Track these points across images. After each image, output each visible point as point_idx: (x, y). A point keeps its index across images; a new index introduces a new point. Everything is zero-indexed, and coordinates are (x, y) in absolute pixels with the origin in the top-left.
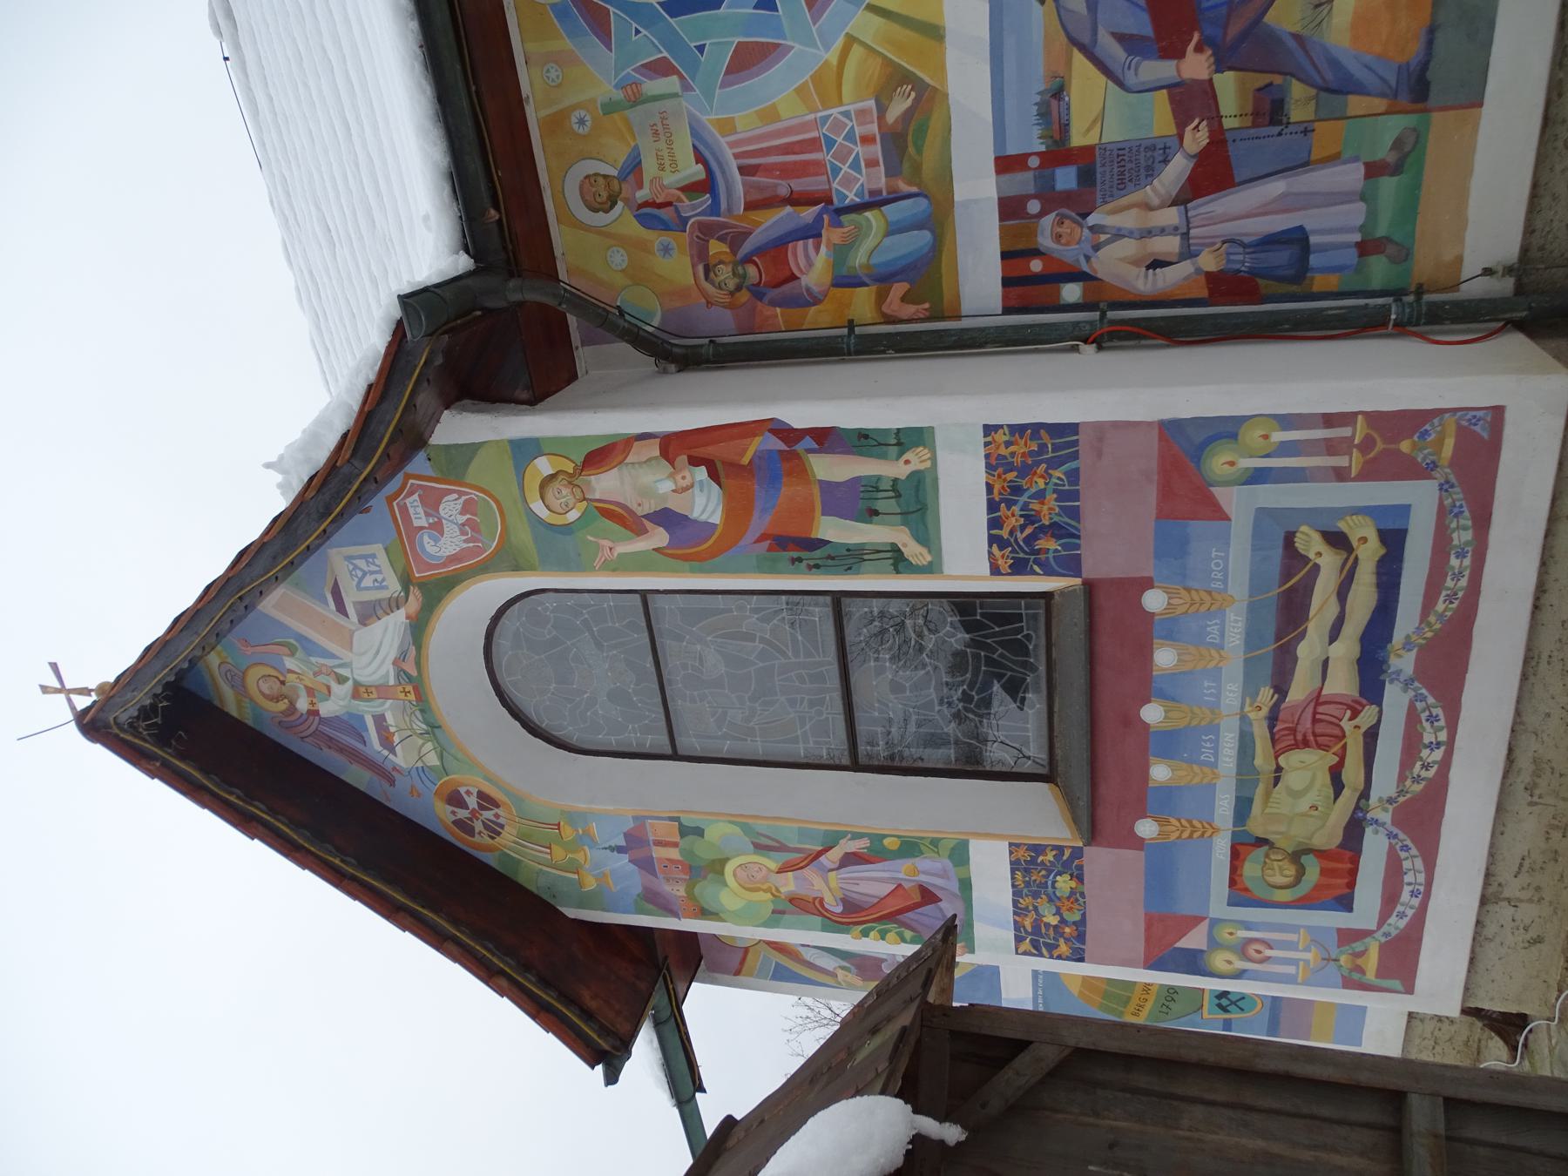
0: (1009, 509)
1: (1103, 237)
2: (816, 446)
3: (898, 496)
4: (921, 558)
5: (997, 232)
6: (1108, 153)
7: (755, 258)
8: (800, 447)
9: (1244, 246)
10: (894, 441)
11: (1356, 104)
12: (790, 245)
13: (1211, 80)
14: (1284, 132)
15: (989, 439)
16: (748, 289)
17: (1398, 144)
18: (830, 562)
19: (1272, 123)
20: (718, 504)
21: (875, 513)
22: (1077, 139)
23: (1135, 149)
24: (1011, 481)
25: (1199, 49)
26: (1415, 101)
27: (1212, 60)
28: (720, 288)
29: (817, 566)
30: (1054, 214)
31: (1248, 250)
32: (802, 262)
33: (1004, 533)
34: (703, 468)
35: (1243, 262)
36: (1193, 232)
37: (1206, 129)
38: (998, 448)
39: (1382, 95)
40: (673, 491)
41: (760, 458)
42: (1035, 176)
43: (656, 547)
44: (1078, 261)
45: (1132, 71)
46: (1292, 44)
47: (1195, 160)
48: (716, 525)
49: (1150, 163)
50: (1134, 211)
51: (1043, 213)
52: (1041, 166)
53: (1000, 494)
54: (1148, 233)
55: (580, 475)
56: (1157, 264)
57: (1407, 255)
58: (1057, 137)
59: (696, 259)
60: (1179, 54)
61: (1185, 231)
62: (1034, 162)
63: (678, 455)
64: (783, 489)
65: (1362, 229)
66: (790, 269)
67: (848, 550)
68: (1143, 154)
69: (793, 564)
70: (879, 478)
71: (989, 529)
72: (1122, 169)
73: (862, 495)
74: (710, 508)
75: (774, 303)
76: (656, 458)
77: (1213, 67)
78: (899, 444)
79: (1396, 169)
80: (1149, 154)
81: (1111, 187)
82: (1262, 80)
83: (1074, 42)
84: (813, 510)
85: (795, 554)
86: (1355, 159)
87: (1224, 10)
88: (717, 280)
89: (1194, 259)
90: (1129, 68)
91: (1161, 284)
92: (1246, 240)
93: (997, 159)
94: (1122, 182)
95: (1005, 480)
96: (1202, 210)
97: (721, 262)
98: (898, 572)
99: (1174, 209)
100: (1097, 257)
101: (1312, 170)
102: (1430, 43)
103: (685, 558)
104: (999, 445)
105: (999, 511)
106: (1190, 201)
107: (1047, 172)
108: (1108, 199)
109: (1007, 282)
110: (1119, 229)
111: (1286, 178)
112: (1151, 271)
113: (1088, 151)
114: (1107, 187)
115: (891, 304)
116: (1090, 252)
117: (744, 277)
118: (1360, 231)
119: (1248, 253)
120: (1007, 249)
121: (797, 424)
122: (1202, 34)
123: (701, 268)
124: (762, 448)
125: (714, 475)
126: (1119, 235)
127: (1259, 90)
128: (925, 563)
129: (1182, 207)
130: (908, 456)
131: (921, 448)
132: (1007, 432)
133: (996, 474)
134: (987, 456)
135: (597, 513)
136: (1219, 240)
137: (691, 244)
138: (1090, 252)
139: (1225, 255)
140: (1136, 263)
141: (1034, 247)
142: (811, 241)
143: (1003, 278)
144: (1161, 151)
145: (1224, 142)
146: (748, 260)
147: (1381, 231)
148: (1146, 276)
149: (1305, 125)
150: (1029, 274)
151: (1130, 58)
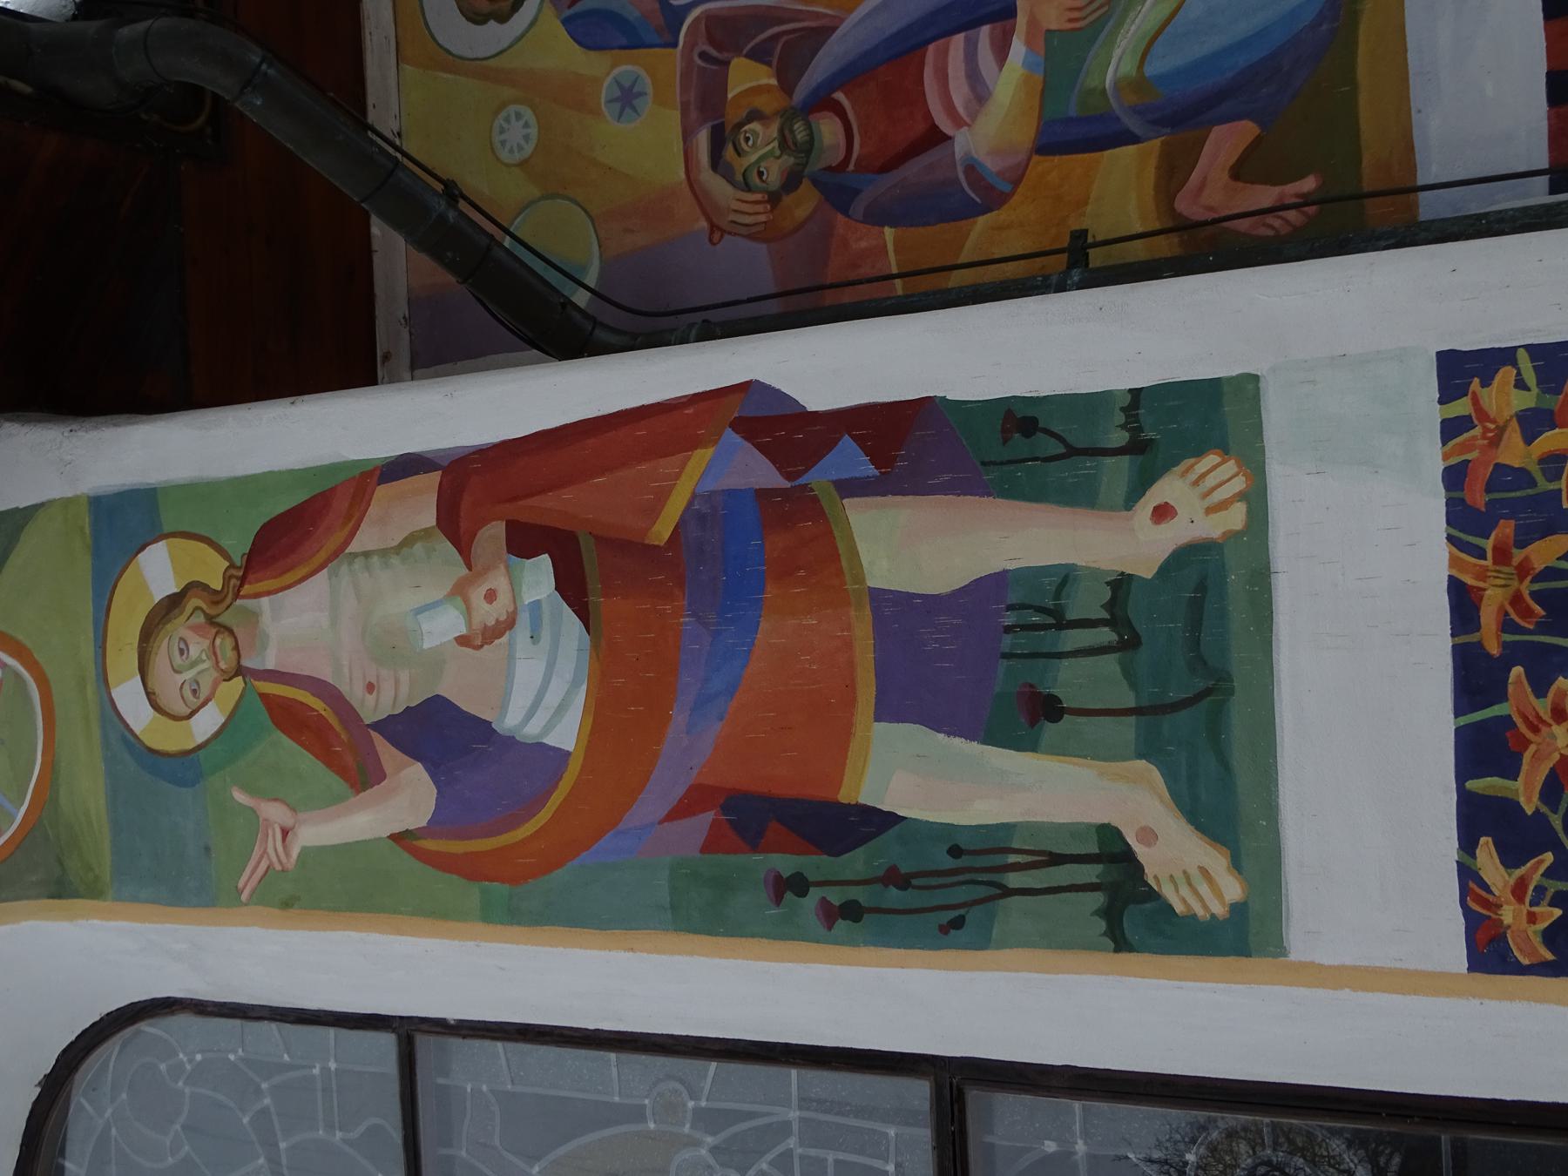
0: (1540, 690)
2: (871, 470)
3: (1129, 643)
4: (1204, 889)
7: (840, 96)
8: (819, 477)
10: (1119, 438)
12: (931, 48)
15: (1462, 407)
16: (815, 182)
18: (894, 896)
20: (575, 684)
21: (1045, 708)
24: (1550, 573)
28: (748, 188)
29: (852, 912)
32: (960, 93)
33: (1525, 791)
34: (545, 560)
38: (1495, 442)
40: (463, 641)
41: (702, 518)
43: (397, 828)
48: (568, 754)
53: (1507, 625)
55: (237, 596)
59: (694, 115)
63: (485, 521)
64: (764, 625)
66: (928, 115)
67: (955, 851)
69: (778, 899)
70: (1066, 577)
71: (1462, 774)
73: (1007, 642)
74: (552, 698)
75: (878, 216)
76: (425, 534)
78: (1137, 447)
84: (850, 702)
85: (785, 863)
88: (741, 164)
95: (1523, 570)
97: (755, 115)
98: (1121, 944)
103: (471, 869)
104: (1501, 430)
105: (1502, 697)
115: (1202, 186)
117: (808, 148)
121: (817, 400)
123: (703, 138)
124: (710, 486)
125: (571, 587)
128: (1219, 910)
130: (1168, 489)
131: (1212, 459)
132: (1530, 377)
133: (1488, 545)
134: (1454, 477)
135: (265, 717)
137: (686, 75)
142: (985, 30)
143: (1549, 74)
146: (821, 101)
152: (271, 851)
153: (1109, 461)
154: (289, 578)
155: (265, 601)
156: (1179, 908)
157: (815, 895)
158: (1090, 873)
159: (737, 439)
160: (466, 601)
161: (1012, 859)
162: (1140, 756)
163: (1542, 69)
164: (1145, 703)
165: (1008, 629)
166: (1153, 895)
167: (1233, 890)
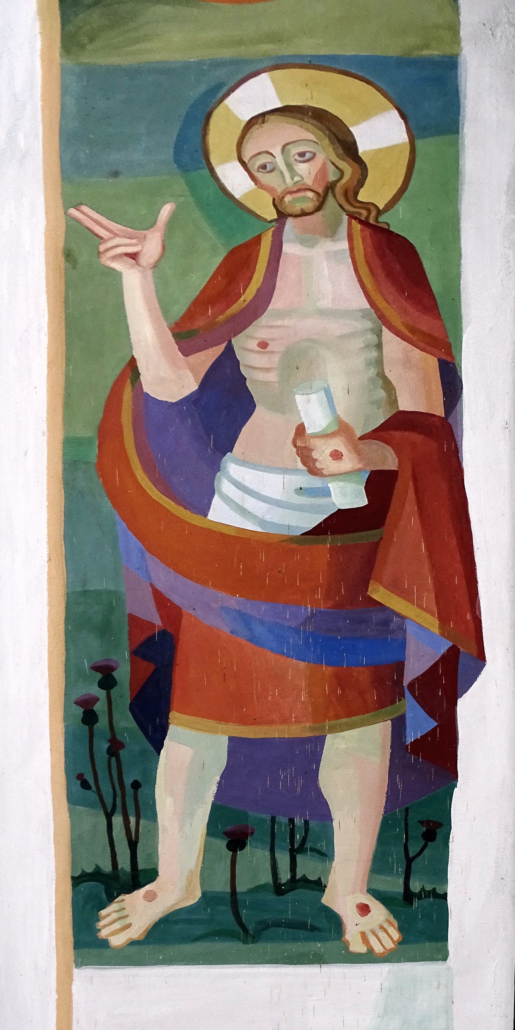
2: (410, 739)
4: (117, 926)
10: (415, 887)
18: (102, 746)
20: (262, 522)
34: (362, 501)
40: (301, 430)
41: (386, 623)
43: (141, 365)
48: (206, 515)
55: (352, 216)
63: (398, 453)
67: (136, 785)
69: (96, 668)
73: (285, 820)
74: (251, 504)
76: (393, 400)
78: (408, 896)
84: (243, 721)
98: (77, 881)
124: (410, 629)
128: (103, 933)
131: (396, 936)
135: (240, 240)
152: (117, 241)
153: (401, 881)
154: (364, 270)
155: (345, 245)
156: (103, 912)
157: (101, 694)
158: (124, 863)
159: (443, 650)
160: (333, 435)
161: (132, 820)
162: (204, 894)
164: (239, 897)
165: (292, 821)
166: (111, 899)
167: (117, 941)
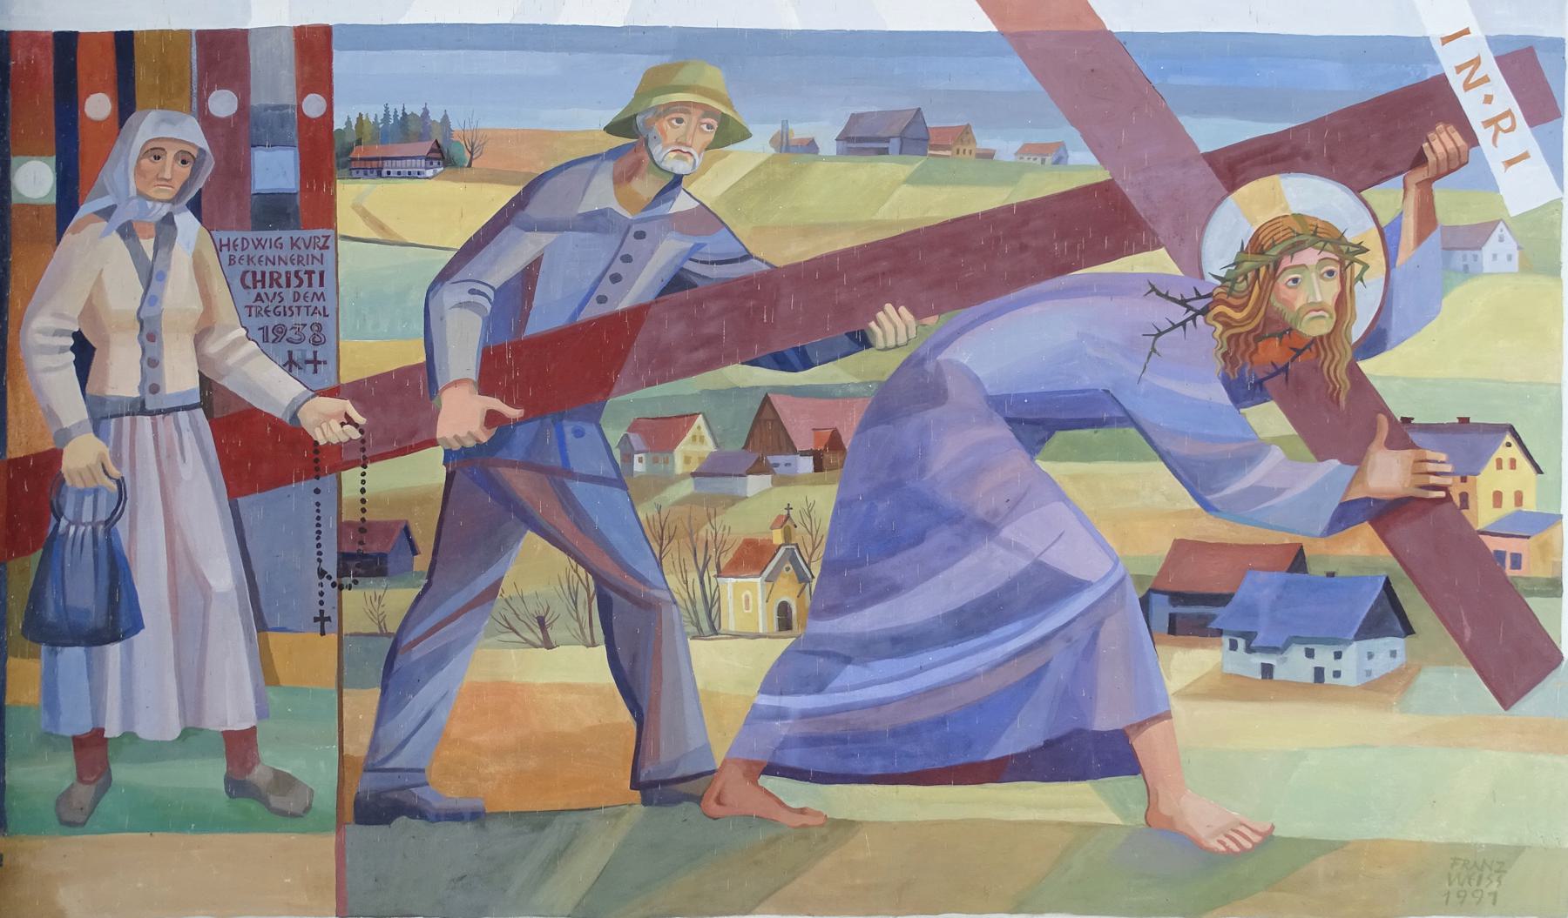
1: (148, 245)
5: (176, 25)
6: (317, 252)
9: (110, 523)
11: (363, 703)
13: (433, 443)
14: (325, 580)
17: (284, 782)
19: (344, 558)
22: (349, 193)
23: (320, 304)
25: (492, 418)
26: (357, 803)
27: (470, 443)
30: (204, 144)
31: (101, 528)
35: (77, 522)
36: (145, 422)
37: (344, 439)
39: (374, 746)
42: (287, 107)
44: (104, 193)
45: (467, 297)
46: (482, 583)
47: (287, 420)
49: (290, 334)
50: (197, 306)
51: (208, 122)
52: (303, 119)
54: (149, 333)
56: (84, 352)
57: (71, 824)
58: (357, 153)
60: (488, 382)
61: (149, 407)
62: (314, 106)
65: (129, 736)
68: (309, 320)
72: (283, 281)
77: (456, 446)
79: (237, 786)
80: (308, 333)
81: (250, 260)
82: (424, 537)
83: (533, 186)
86: (262, 713)
87: (555, 461)
89: (89, 426)
90: (472, 292)
91: (40, 362)
92: (122, 527)
93: (327, 31)
94: (259, 280)
96: (188, 437)
99: (193, 383)
100: (106, 233)
101: (249, 639)
102: (456, 816)
106: (209, 415)
107: (292, 132)
108: (225, 253)
109: (66, 43)
110: (162, 277)
111: (238, 588)
112: (71, 342)
113: (324, 213)
114: (251, 250)
116: (119, 218)
118: (124, 735)
119: (94, 531)
120: (136, 36)
122: (517, 423)
126: (151, 276)
127: (407, 531)
129: (197, 400)
136: (125, 472)
138: (119, 218)
139: (92, 485)
140: (91, 311)
141: (139, 101)
143: (76, 33)
144: (310, 356)
145: (316, 471)
147: (122, 772)
148: (59, 333)
149: (335, 619)
150: (81, 93)
151: (491, 294)
163: (80, 30)
